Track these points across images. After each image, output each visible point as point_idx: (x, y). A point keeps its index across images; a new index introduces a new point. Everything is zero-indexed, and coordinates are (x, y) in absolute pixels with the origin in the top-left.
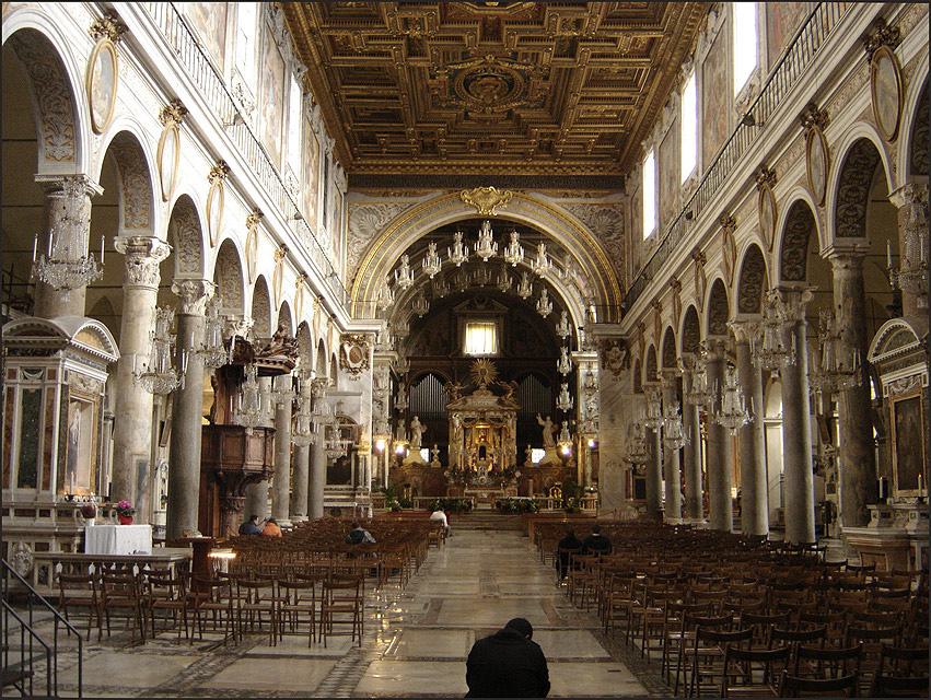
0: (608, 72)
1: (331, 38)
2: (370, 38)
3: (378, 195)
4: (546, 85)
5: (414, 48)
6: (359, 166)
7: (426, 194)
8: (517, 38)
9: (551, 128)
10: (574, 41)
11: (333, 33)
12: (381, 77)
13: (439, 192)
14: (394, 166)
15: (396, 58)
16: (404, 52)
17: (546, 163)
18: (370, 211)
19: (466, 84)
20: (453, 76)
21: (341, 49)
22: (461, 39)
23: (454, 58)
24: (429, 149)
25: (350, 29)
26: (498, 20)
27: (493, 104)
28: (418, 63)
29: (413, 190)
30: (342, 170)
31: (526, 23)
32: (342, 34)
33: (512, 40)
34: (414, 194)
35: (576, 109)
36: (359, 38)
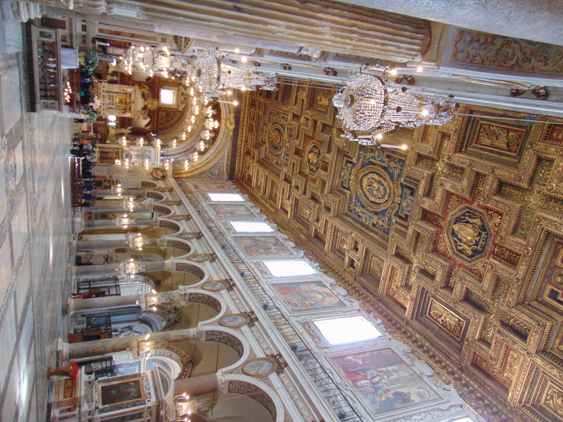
4: (274, 162)
9: (256, 159)
10: (290, 182)
31: (300, 168)
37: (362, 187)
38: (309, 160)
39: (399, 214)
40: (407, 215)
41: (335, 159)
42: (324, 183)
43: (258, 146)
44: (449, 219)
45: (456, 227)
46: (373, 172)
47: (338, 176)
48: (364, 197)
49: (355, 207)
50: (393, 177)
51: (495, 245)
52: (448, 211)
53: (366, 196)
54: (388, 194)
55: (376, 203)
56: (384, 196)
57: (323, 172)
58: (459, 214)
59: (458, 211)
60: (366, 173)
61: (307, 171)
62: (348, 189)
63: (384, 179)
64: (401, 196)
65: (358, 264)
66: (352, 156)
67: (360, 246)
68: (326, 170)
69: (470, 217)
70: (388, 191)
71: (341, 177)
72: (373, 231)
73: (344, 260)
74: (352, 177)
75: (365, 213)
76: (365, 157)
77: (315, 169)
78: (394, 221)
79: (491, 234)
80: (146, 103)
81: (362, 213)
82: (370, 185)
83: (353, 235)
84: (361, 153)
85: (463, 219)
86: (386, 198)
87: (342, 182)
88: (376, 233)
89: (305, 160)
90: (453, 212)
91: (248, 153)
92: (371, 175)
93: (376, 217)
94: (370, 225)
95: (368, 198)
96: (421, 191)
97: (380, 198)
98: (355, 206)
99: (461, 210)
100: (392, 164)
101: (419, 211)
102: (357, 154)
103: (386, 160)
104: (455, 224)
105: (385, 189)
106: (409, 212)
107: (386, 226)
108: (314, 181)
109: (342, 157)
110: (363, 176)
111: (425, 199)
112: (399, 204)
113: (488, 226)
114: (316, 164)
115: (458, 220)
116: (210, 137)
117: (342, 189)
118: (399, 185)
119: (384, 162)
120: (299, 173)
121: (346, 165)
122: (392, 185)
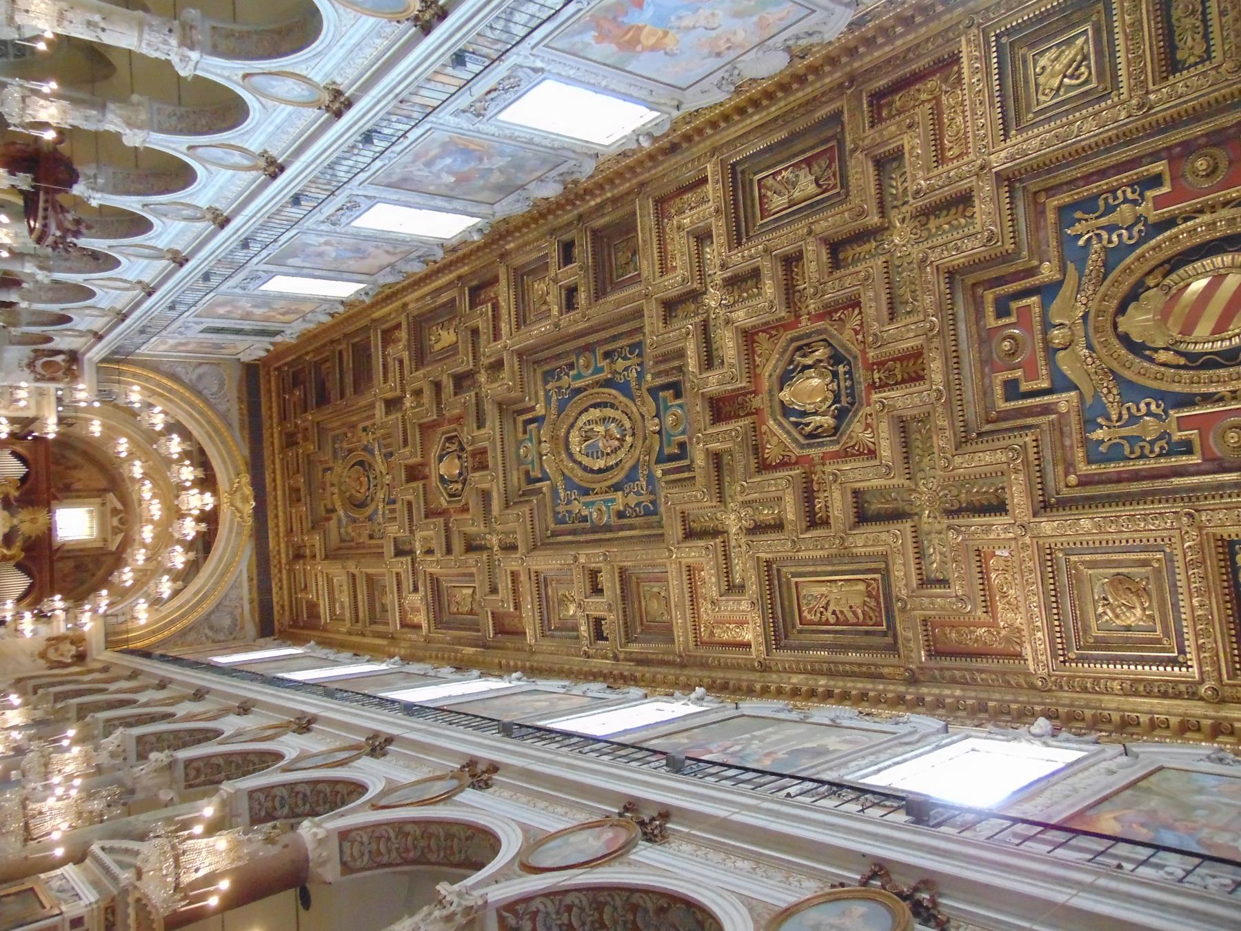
0: (384, 593)
1: (398, 326)
2: (401, 362)
3: (239, 391)
5: (392, 404)
6: (268, 373)
7: (243, 438)
8: (410, 497)
11: (404, 326)
12: (362, 378)
13: (247, 452)
14: (270, 408)
15: (382, 388)
16: (389, 395)
17: (283, 556)
18: (222, 385)
19: (361, 463)
20: (365, 449)
21: (388, 337)
22: (405, 443)
23: (386, 446)
24: (290, 441)
25: (409, 340)
26: (425, 477)
27: (342, 493)
28: (380, 409)
29: (247, 426)
30: (263, 354)
31: (426, 503)
32: (403, 334)
33: (409, 493)
34: (242, 428)
35: (338, 571)
36: (400, 349)
37: (571, 455)
38: (441, 477)
39: (667, 451)
40: (682, 445)
41: (498, 430)
42: (486, 496)
43: (317, 524)
44: (766, 385)
45: (785, 395)
46: (586, 410)
47: (515, 467)
48: (580, 472)
49: (569, 507)
50: (629, 388)
51: (870, 368)
52: (758, 371)
53: (586, 469)
54: (629, 432)
55: (612, 468)
56: (622, 440)
57: (477, 474)
58: (781, 364)
59: (779, 360)
60: (571, 420)
61: (443, 502)
62: (545, 477)
63: (612, 406)
64: (657, 415)
65: (612, 619)
66: (533, 403)
67: (605, 580)
68: (485, 467)
69: (804, 356)
70: (628, 424)
71: (520, 461)
72: (622, 528)
73: (577, 637)
74: (545, 447)
75: (593, 503)
76: (559, 388)
77: (459, 486)
78: (659, 473)
79: (855, 357)
80: (15, 521)
81: (587, 505)
82: (587, 439)
83: (582, 560)
84: (548, 387)
85: (793, 370)
86: (629, 439)
87: (527, 473)
88: (631, 527)
89: (434, 480)
90: (769, 368)
91: (299, 556)
92: (584, 418)
93: (620, 493)
94: (614, 521)
95: (592, 471)
96: (692, 364)
97: (615, 451)
98: (569, 502)
99: (782, 354)
100: (620, 364)
101: (704, 409)
102: (542, 393)
103: (604, 363)
104: (781, 389)
105: (620, 425)
106: (683, 433)
107: (645, 499)
108: (465, 509)
109: (511, 421)
110: (568, 432)
111: (705, 375)
112: (659, 432)
113: (843, 346)
114: (460, 474)
115: (785, 379)
116: (198, 532)
117: (531, 487)
118: (646, 394)
119: (601, 370)
120: (427, 517)
121: (525, 432)
122: (631, 404)
